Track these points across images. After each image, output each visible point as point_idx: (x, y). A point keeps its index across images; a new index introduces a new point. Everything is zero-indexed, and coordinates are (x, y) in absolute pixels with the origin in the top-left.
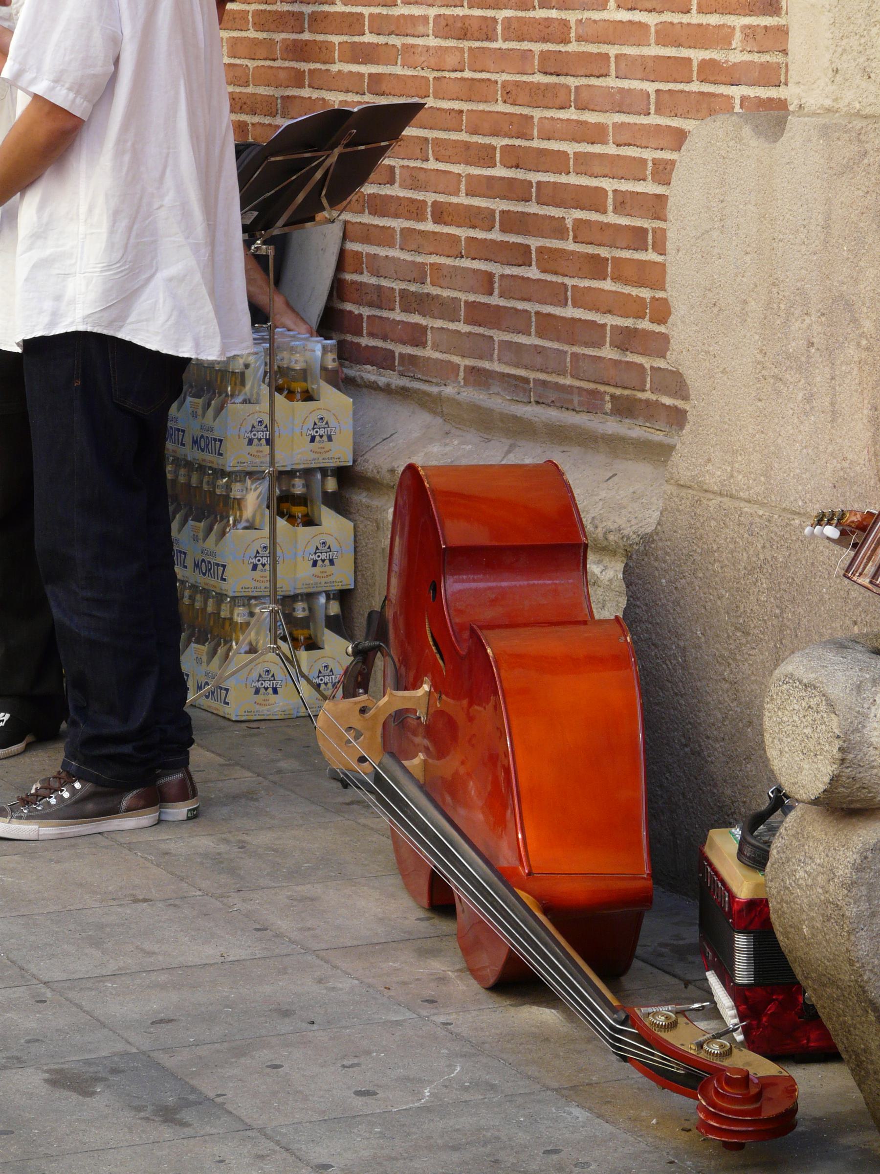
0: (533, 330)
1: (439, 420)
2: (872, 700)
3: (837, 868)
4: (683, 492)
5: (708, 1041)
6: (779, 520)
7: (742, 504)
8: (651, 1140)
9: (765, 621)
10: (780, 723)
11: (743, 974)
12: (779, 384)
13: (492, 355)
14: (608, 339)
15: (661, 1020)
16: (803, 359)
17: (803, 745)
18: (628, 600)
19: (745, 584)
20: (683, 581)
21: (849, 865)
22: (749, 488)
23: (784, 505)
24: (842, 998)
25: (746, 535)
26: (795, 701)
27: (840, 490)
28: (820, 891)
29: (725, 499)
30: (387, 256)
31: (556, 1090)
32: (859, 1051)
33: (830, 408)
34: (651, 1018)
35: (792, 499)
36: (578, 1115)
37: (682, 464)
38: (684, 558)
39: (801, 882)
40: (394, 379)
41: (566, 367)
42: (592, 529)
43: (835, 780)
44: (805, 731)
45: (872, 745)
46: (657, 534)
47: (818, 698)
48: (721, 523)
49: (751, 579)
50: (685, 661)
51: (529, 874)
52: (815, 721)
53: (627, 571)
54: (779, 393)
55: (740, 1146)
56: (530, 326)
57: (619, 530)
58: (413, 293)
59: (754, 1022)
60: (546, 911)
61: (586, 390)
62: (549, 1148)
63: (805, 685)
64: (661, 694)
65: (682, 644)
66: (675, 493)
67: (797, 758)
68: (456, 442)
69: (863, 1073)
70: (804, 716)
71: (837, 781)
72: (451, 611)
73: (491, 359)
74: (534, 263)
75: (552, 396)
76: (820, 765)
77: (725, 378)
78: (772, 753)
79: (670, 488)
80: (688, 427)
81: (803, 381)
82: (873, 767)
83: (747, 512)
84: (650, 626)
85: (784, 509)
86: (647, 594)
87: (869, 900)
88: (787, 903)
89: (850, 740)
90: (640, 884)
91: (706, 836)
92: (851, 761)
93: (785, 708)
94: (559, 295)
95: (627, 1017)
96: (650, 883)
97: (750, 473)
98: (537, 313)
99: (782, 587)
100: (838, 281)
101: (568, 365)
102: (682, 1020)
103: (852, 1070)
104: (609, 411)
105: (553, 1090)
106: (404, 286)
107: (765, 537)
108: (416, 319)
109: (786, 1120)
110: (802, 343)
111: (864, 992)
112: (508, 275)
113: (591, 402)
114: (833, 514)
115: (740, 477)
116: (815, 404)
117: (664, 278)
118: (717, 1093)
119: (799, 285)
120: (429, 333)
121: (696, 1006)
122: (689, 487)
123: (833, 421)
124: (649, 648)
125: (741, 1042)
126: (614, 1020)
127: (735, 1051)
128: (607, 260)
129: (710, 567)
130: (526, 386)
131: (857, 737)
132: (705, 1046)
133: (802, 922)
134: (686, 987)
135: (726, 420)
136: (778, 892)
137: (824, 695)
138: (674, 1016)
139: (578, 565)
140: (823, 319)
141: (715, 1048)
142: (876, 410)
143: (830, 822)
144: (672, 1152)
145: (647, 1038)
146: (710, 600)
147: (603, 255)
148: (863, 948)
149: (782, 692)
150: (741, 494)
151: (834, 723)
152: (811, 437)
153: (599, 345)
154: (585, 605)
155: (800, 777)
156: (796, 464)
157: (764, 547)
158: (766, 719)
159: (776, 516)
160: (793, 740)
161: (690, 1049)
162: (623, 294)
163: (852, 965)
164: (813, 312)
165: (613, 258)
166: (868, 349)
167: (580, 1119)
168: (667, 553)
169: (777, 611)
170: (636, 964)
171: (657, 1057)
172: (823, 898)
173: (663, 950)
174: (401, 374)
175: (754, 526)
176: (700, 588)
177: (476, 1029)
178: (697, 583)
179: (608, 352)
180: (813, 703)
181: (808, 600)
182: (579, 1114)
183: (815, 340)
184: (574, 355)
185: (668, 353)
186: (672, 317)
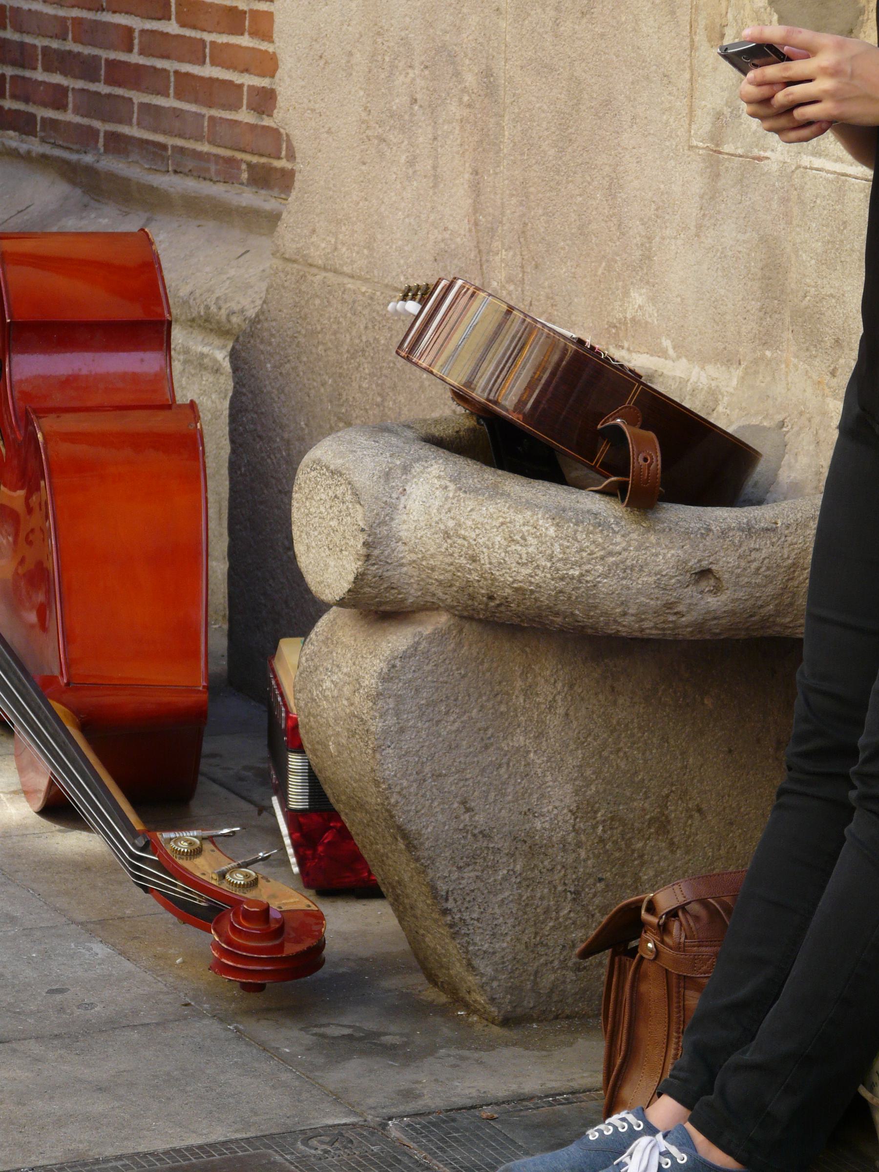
0: (172, 91)
1: (78, 192)
2: (401, 489)
3: (364, 678)
4: (289, 266)
5: (232, 870)
6: (381, 298)
7: (346, 280)
8: (171, 980)
9: (366, 410)
10: (307, 515)
11: (298, 798)
12: (383, 146)
13: (131, 119)
14: (245, 102)
15: (183, 846)
16: (407, 117)
17: (329, 539)
18: (235, 387)
19: (348, 369)
20: (288, 366)
21: (375, 674)
22: (353, 262)
23: (386, 281)
24: (371, 824)
25: (349, 315)
26: (322, 490)
27: (441, 264)
28: (345, 703)
29: (330, 275)
30: (30, 10)
31: (82, 924)
32: (395, 884)
33: (432, 172)
34: (172, 843)
35: (394, 274)
36: (98, 951)
37: (290, 234)
38: (288, 340)
39: (328, 693)
40: (34, 146)
41: (203, 131)
42: (215, 310)
43: (360, 578)
44: (331, 523)
45: (400, 540)
46: (263, 313)
47: (343, 486)
48: (325, 301)
49: (354, 363)
50: (289, 455)
51: (68, 684)
52: (340, 512)
53: (234, 356)
54: (382, 155)
55: (260, 988)
56: (168, 87)
57: (242, 311)
58: (55, 51)
59: (309, 852)
60: (84, 727)
61: (223, 158)
62: (54, 987)
63: (332, 472)
64: (265, 491)
65: (286, 436)
66: (280, 268)
67: (323, 554)
68: (93, 216)
69: (401, 908)
70: (331, 507)
71: (362, 580)
72: (16, 394)
73: (130, 123)
74: (173, 17)
75: (190, 164)
76: (345, 563)
77: (330, 140)
78: (299, 548)
79: (277, 263)
80: (294, 194)
81: (406, 142)
82: (402, 565)
83: (350, 289)
84: (255, 416)
85: (387, 286)
86: (253, 380)
87: (397, 715)
88: (315, 716)
89: (375, 534)
90: (192, 699)
91: (275, 647)
92: (378, 557)
93: (312, 498)
94: (196, 52)
95: (148, 843)
96: (205, 697)
97: (354, 245)
98: (176, 72)
99: (385, 372)
100: (442, 30)
101: (206, 129)
102: (207, 846)
103: (392, 905)
104: (245, 181)
105: (78, 924)
106: (46, 42)
107: (367, 316)
108: (57, 79)
109: (312, 958)
110: (406, 99)
111: (392, 817)
112: (147, 30)
113: (227, 170)
114: (418, 288)
115: (344, 249)
116: (417, 168)
117: (272, 26)
118: (233, 928)
119: (403, 34)
120: (70, 95)
121: (226, 831)
122: (295, 261)
123: (435, 186)
124: (254, 440)
125: (297, 875)
126: (134, 845)
127: (262, 882)
128: (245, 12)
129: (314, 350)
130: (164, 153)
131: (384, 530)
132: (228, 876)
133: (328, 738)
134: (260, 813)
135: (331, 186)
136: (306, 705)
137: (349, 484)
138: (198, 842)
139: (162, 345)
140: (427, 72)
141: (239, 878)
142: (477, 174)
143: (361, 626)
144: (191, 993)
145: (168, 866)
146: (314, 388)
147: (241, 8)
148: (390, 767)
149: (310, 481)
150: (345, 269)
151: (359, 516)
152: (413, 204)
153: (236, 107)
154: (167, 389)
155: (326, 576)
156: (399, 235)
157: (366, 328)
158: (294, 510)
159: (378, 293)
160: (320, 533)
161: (212, 879)
162: (260, 51)
163: (378, 786)
164: (416, 64)
165: (251, 11)
166: (469, 106)
167: (99, 956)
168: (272, 335)
169: (379, 399)
170: (204, 786)
171: (179, 888)
172: (348, 711)
173: (246, 773)
174: (43, 141)
175: (356, 305)
176: (304, 373)
177: (13, 856)
178: (301, 368)
179: (245, 116)
180: (339, 492)
181: (408, 387)
182: (100, 950)
183: (418, 96)
184: (212, 119)
185: (275, 111)
186: (280, 70)
